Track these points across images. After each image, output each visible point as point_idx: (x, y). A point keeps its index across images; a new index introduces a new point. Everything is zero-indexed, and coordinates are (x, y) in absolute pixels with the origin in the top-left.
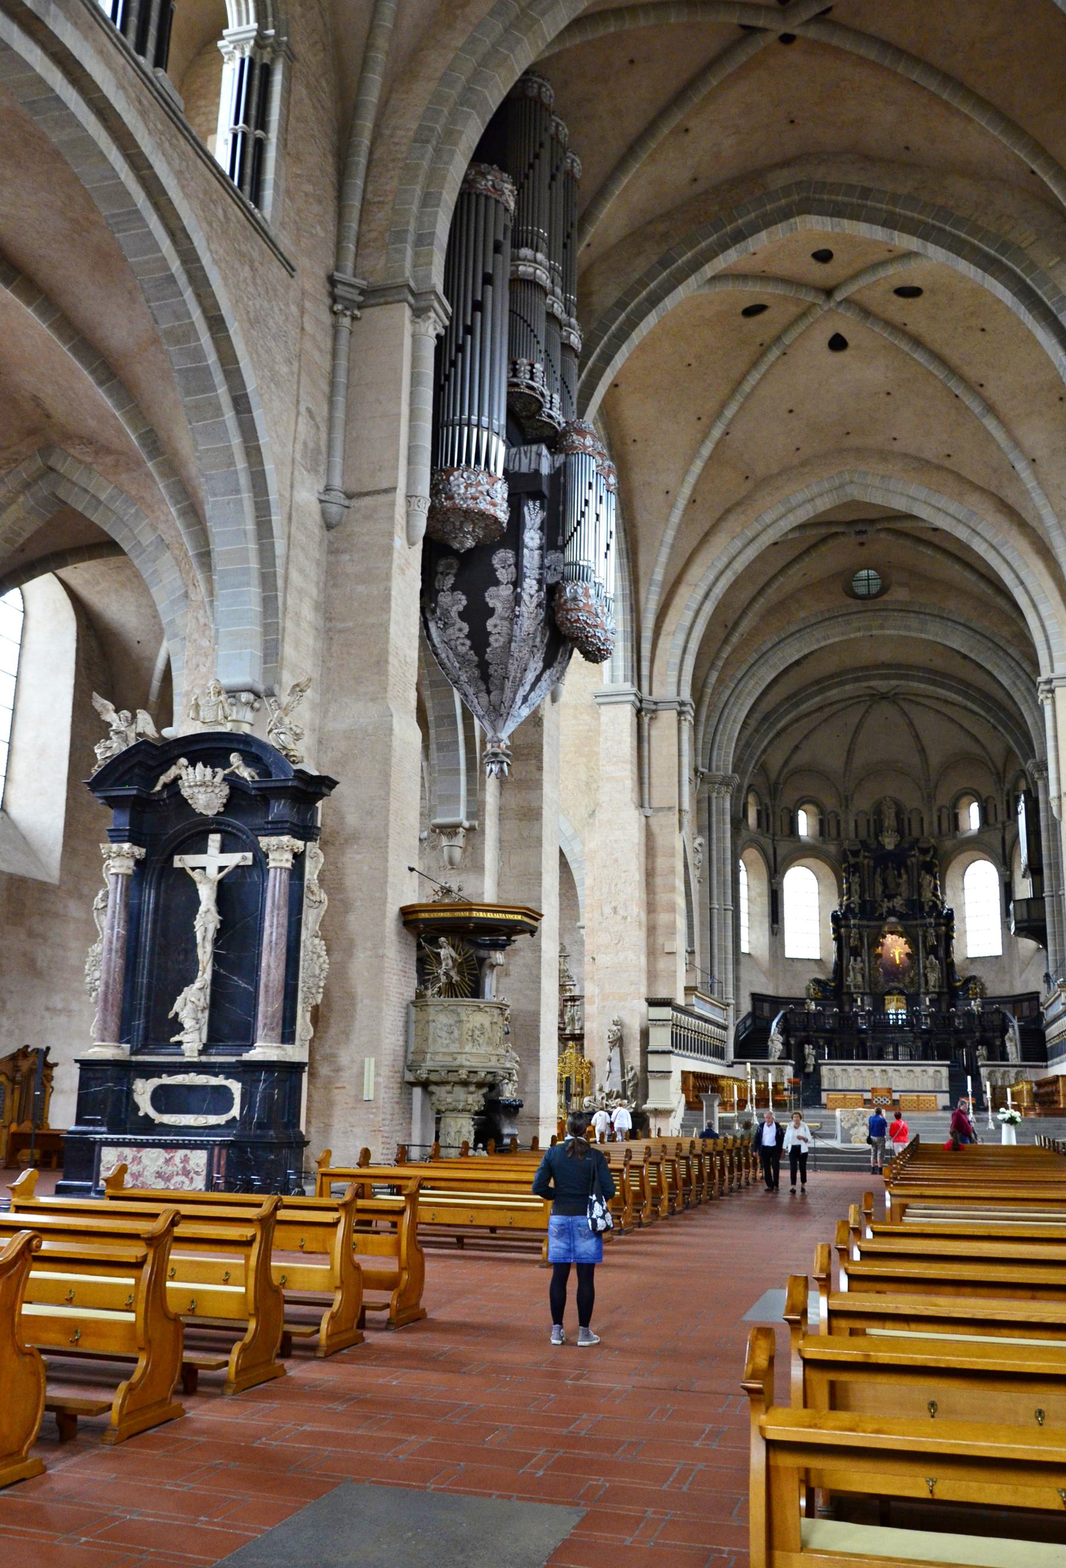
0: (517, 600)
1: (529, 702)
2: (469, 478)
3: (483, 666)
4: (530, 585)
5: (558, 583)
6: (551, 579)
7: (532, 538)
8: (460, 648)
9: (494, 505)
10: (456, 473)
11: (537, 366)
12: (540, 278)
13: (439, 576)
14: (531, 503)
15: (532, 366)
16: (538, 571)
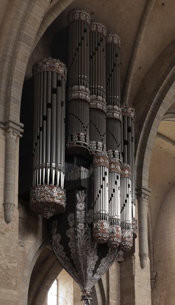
0: (76, 233)
1: (98, 273)
2: (41, 189)
3: (72, 261)
4: (81, 226)
5: (92, 222)
6: (90, 222)
7: (81, 206)
8: (63, 256)
9: (53, 198)
10: (36, 189)
11: (82, 134)
12: (82, 96)
13: (53, 229)
14: (80, 192)
15: (79, 134)
16: (84, 219)
